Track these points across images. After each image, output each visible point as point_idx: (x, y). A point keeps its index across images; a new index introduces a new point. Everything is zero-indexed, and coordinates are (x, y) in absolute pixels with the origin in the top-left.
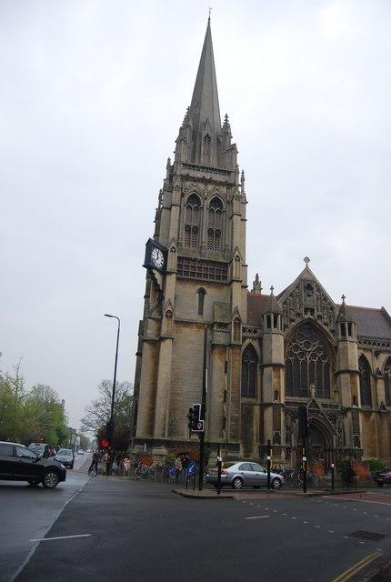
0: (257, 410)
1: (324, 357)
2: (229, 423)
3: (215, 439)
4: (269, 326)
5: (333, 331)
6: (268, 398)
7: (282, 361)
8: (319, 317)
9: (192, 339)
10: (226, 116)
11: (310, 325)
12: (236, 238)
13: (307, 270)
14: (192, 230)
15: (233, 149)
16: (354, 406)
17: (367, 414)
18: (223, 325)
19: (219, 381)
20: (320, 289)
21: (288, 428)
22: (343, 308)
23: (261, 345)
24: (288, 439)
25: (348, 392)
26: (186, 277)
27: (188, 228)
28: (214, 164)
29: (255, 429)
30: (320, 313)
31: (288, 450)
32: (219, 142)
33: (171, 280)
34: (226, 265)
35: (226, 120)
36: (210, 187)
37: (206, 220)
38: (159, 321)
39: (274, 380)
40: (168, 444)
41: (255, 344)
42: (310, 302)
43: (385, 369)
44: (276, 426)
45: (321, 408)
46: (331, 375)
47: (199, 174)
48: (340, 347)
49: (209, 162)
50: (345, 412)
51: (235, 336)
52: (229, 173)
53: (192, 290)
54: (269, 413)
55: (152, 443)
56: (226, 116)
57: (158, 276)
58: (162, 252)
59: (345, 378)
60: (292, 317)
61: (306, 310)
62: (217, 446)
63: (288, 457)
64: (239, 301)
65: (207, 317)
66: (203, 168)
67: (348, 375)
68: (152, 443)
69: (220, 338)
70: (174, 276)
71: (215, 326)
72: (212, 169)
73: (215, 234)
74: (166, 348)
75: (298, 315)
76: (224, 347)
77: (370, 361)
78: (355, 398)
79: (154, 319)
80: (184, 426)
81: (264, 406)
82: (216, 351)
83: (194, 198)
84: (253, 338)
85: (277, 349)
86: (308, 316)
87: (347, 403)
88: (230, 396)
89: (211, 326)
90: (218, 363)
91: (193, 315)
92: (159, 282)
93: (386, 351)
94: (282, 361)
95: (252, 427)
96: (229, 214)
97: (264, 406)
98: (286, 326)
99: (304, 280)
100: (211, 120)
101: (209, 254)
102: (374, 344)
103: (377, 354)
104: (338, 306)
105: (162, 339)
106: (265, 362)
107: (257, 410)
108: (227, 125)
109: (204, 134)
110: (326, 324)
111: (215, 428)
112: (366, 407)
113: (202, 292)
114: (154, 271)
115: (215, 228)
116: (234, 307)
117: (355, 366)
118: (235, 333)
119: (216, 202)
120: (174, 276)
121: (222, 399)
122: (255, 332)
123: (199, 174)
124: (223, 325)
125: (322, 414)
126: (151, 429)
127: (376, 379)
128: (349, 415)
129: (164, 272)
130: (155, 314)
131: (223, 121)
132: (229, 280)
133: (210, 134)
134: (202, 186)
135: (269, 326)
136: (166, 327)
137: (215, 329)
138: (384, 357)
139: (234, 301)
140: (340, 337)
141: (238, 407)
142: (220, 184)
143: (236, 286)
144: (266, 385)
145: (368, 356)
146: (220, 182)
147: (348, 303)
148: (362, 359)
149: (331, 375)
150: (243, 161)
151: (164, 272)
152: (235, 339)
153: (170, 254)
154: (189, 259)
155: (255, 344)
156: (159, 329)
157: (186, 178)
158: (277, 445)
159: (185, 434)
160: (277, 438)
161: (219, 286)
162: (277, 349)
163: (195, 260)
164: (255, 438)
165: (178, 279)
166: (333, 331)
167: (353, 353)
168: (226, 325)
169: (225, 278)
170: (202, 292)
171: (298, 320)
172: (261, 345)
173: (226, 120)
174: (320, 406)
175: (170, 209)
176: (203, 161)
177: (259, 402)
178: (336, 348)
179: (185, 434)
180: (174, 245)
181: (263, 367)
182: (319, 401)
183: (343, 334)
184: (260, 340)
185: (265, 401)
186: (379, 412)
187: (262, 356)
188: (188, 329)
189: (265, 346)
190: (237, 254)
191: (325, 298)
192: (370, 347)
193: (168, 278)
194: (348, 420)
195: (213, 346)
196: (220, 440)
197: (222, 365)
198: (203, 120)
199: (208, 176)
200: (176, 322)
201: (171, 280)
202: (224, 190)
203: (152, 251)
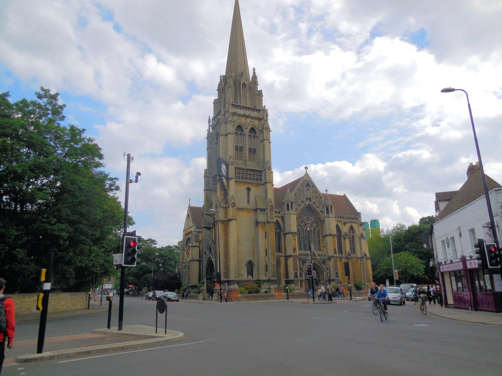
0: (282, 260)
1: (317, 226)
2: (270, 268)
3: (263, 278)
4: (288, 210)
5: (321, 211)
6: (290, 252)
7: (296, 231)
8: (314, 203)
9: (246, 219)
10: (254, 69)
11: (309, 208)
12: (266, 154)
13: (307, 174)
14: (239, 149)
15: (260, 93)
16: (335, 255)
17: (341, 259)
18: (263, 210)
19: (262, 243)
20: (314, 186)
21: (300, 269)
22: (326, 196)
23: (283, 221)
24: (301, 276)
25: (331, 245)
26: (239, 180)
27: (237, 148)
28: (249, 105)
29: (282, 270)
30: (314, 201)
31: (301, 281)
32: (250, 88)
33: (232, 183)
34: (261, 171)
35: (254, 72)
36: (249, 120)
37: (247, 143)
38: (226, 208)
39: (293, 242)
40: (239, 282)
41: (280, 220)
42: (309, 194)
43: (349, 233)
44: (295, 269)
45: (318, 257)
46: (321, 237)
47: (242, 112)
48: (327, 220)
49: (246, 102)
50: (330, 258)
51: (270, 217)
52: (259, 110)
53: (243, 188)
54: (290, 261)
55: (229, 282)
56: (254, 69)
57: (225, 181)
58: (226, 165)
59: (329, 239)
60: (300, 203)
61: (307, 199)
62: (264, 281)
63: (301, 286)
64: (271, 196)
65: (252, 205)
66: (244, 107)
67: (331, 237)
68: (229, 282)
69: (262, 218)
70: (234, 180)
71: (258, 210)
72: (249, 108)
73: (253, 151)
74: (233, 226)
75: (303, 202)
76: (264, 223)
77: (341, 229)
78: (335, 250)
79: (222, 207)
80: (244, 271)
81: (287, 257)
82: (260, 226)
83: (240, 127)
84: (278, 217)
85: (292, 224)
86: (308, 203)
87: (331, 253)
88: (270, 252)
89: (256, 210)
90: (261, 233)
91: (244, 204)
92: (225, 185)
93: (350, 222)
94: (296, 231)
95: (281, 270)
96: (261, 139)
97: (287, 257)
98: (296, 209)
99: (305, 181)
100: (245, 72)
101: (251, 165)
102: (343, 218)
103: (345, 224)
104: (323, 194)
105: (230, 220)
106: (287, 231)
107: (282, 260)
108: (255, 77)
109: (242, 83)
110: (317, 207)
111: (262, 270)
112: (340, 255)
113: (249, 189)
114: (223, 178)
115: (252, 147)
116: (268, 198)
117: (334, 232)
118: (270, 215)
119: (253, 130)
120: (234, 180)
121: (265, 254)
122: (279, 213)
123: (242, 112)
124: (263, 210)
125: (318, 260)
126: (227, 274)
127: (345, 239)
128: (332, 260)
129: (228, 179)
130: (223, 204)
131: (251, 75)
132: (263, 182)
133: (246, 83)
134: (243, 120)
135: (288, 210)
136: (231, 213)
137: (258, 212)
138: (348, 225)
139: (268, 195)
140: (326, 215)
141: (274, 258)
142: (255, 118)
143: (268, 185)
144: (288, 245)
145: (340, 225)
146: (255, 117)
147: (328, 193)
148: (337, 227)
149: (321, 237)
150: (267, 102)
151: (228, 179)
152: (270, 218)
153: (230, 166)
154: (240, 169)
155: (280, 220)
156: (226, 213)
157: (234, 114)
158: (296, 279)
159: (245, 276)
160: (296, 276)
161: (258, 185)
162: (292, 224)
163: (243, 169)
164: (282, 276)
165: (236, 182)
166: (321, 211)
167: (331, 224)
168: (264, 210)
169: (261, 180)
170: (249, 189)
171: (303, 205)
172: (283, 221)
173: (254, 72)
174: (317, 255)
175: (227, 135)
176: (242, 103)
177: (283, 255)
178: (324, 221)
179: (245, 276)
180: (232, 160)
181: (285, 234)
182: (316, 253)
183: (328, 213)
184: (283, 218)
185: (288, 254)
186: (347, 258)
187: (284, 228)
188: (242, 213)
189: (286, 221)
190: (268, 165)
191: (317, 191)
192: (341, 220)
193: (230, 181)
194: (331, 264)
195: (257, 223)
196: (265, 278)
197: (264, 234)
198: (240, 71)
199: (247, 114)
200: (237, 209)
201: (232, 183)
202: (256, 122)
203: (221, 165)
